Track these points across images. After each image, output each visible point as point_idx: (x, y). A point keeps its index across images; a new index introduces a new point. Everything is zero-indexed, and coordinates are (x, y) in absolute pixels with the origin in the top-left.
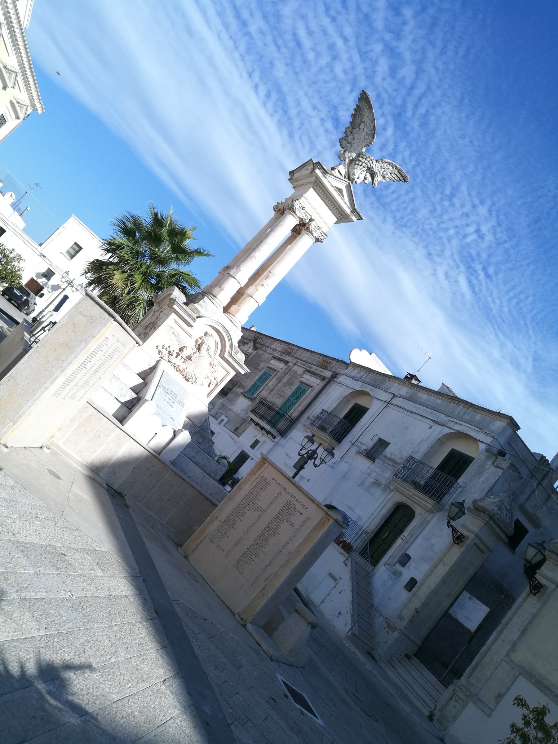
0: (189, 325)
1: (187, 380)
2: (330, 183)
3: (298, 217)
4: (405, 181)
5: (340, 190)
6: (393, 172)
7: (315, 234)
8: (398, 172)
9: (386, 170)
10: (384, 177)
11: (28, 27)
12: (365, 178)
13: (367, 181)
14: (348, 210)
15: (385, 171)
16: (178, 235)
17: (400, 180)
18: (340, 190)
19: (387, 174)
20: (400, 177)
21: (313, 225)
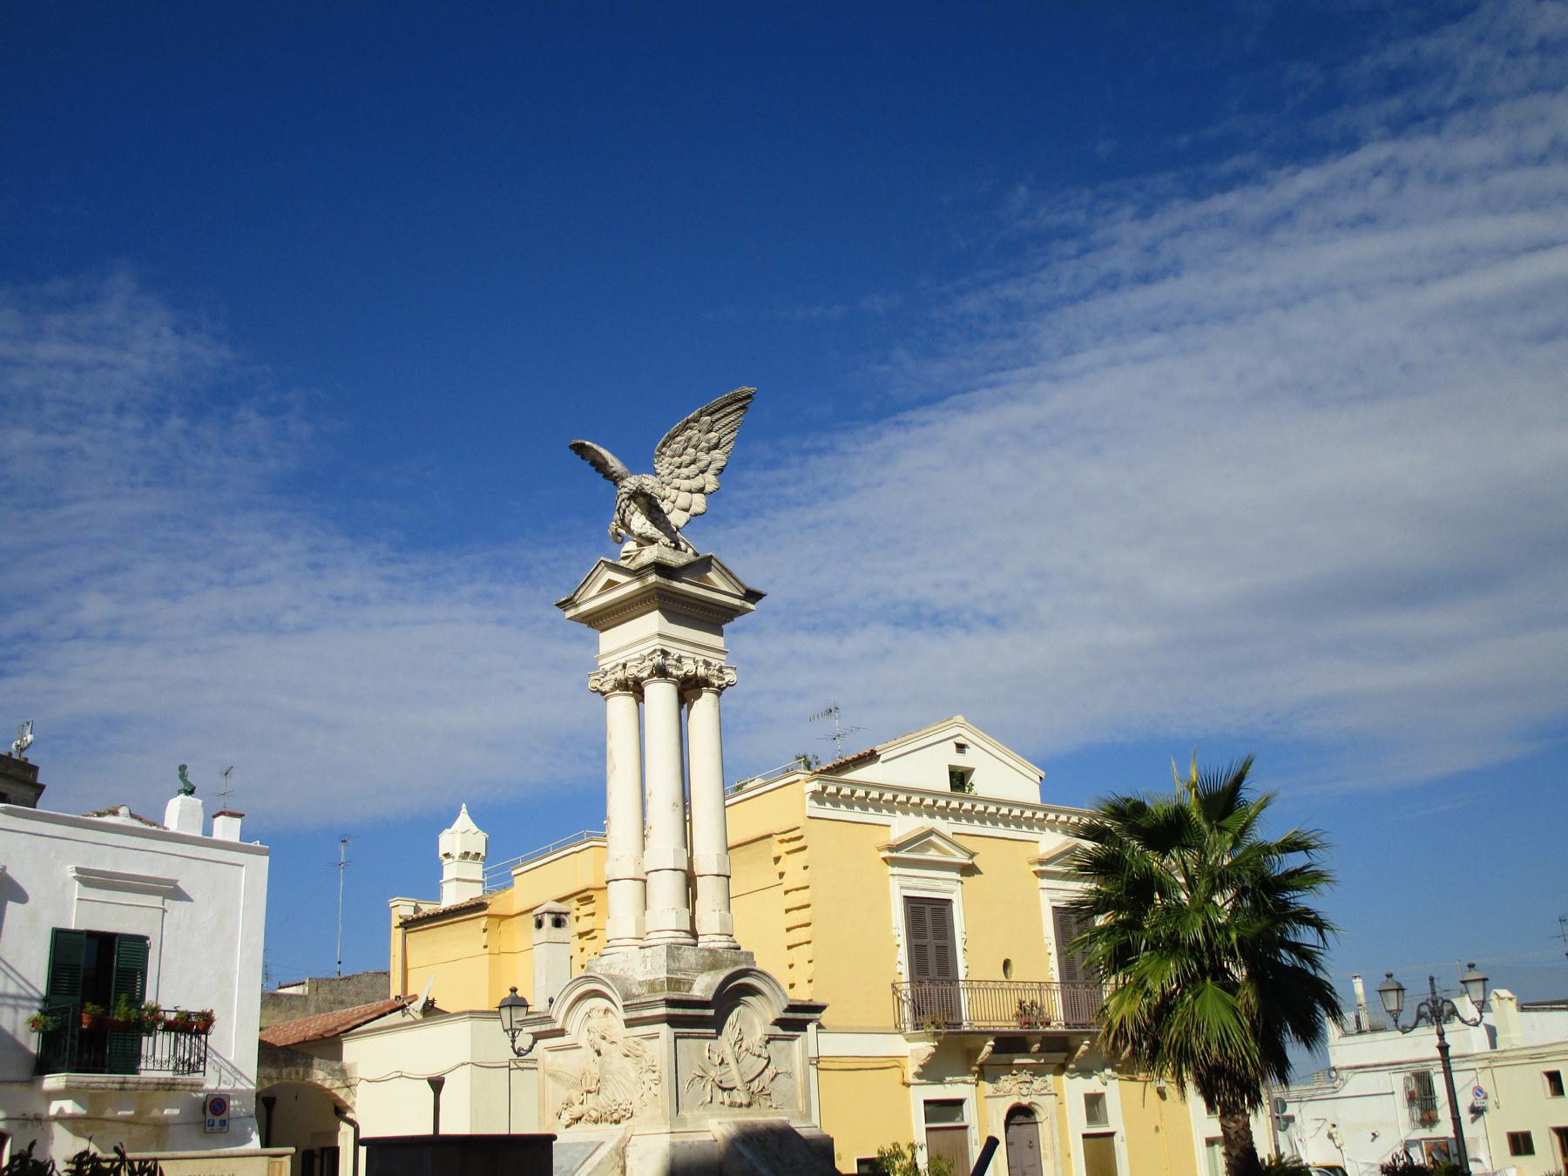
0: (561, 1033)
1: (617, 1122)
2: (592, 601)
3: (613, 689)
4: (749, 397)
5: (611, 584)
6: (705, 427)
7: (645, 674)
8: (710, 414)
9: (694, 442)
10: (716, 447)
11: (1043, 774)
12: (701, 490)
13: (709, 488)
14: (636, 586)
15: (695, 447)
16: (1129, 814)
17: (743, 408)
18: (611, 584)
19: (708, 441)
20: (729, 410)
21: (632, 671)
